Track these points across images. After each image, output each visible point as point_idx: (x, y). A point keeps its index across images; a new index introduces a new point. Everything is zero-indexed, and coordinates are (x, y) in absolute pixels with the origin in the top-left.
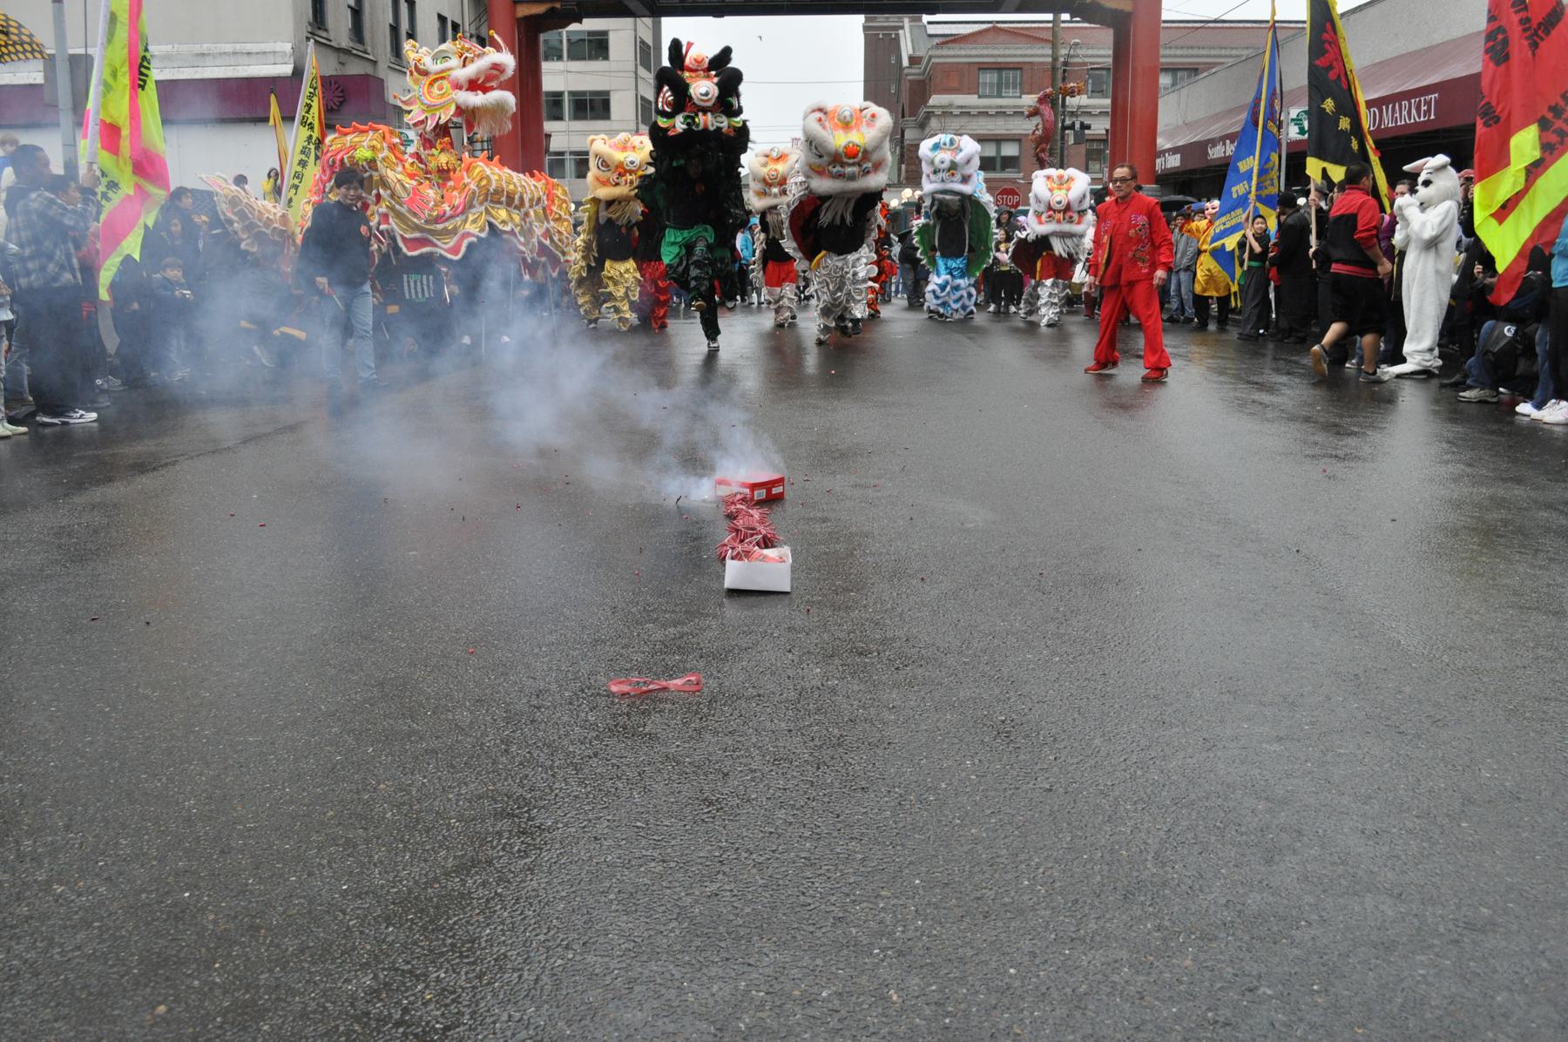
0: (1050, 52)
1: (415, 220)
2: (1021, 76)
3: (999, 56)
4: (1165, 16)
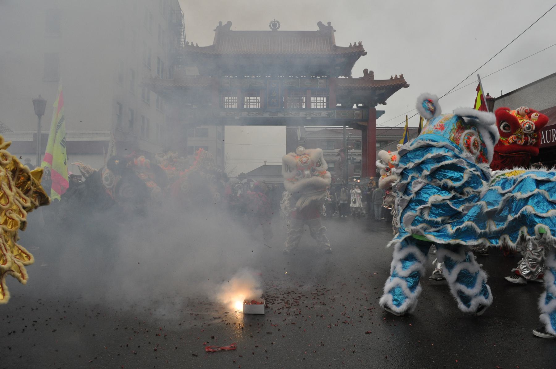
0: (342, 136)
4: (377, 127)
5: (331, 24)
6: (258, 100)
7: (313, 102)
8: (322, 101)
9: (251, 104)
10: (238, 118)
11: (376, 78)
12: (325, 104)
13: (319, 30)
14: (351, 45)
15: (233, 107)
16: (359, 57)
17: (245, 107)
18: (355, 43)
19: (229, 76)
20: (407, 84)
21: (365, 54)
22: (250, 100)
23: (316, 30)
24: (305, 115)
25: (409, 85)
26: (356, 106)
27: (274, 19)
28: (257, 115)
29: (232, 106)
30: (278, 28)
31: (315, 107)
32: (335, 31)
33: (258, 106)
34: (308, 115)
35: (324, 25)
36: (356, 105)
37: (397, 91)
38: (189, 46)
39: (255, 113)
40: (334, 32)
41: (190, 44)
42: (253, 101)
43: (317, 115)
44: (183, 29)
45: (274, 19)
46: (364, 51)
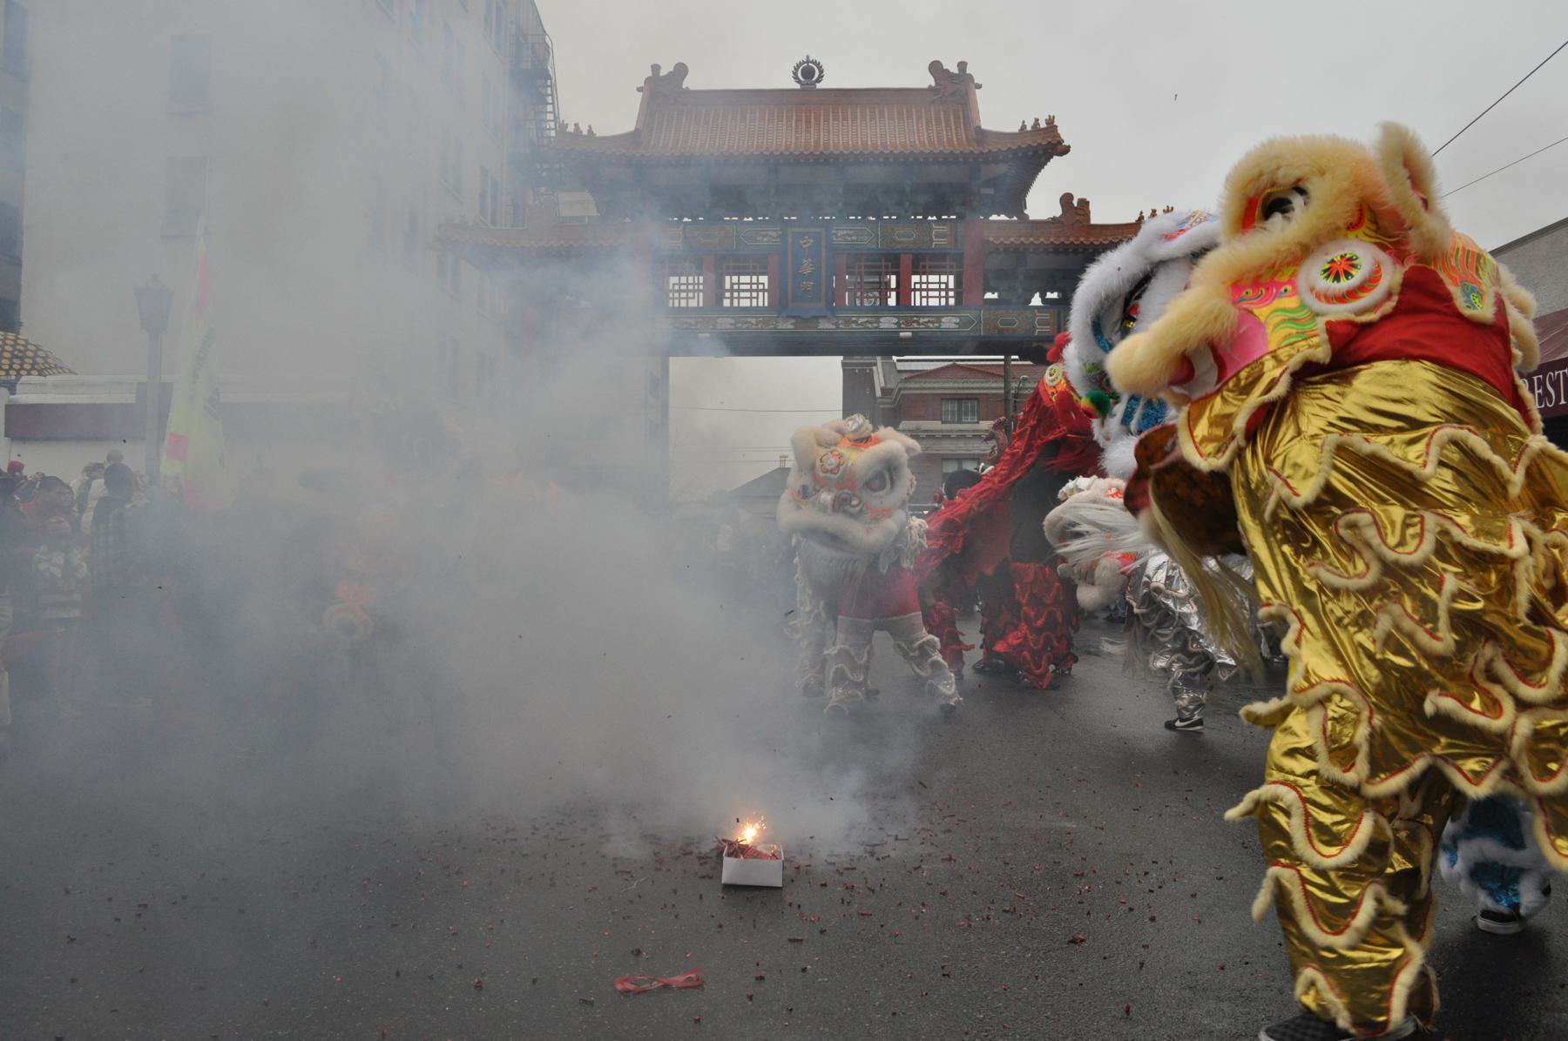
0: (1003, 385)
2: (978, 403)
3: (959, 388)
5: (968, 66)
6: (763, 284)
7: (918, 290)
8: (943, 286)
9: (742, 294)
11: (1095, 219)
12: (951, 294)
13: (933, 84)
14: (1024, 127)
15: (693, 303)
16: (1048, 160)
17: (727, 303)
18: (1037, 120)
19: (681, 218)
21: (1066, 150)
22: (739, 284)
23: (926, 86)
24: (896, 326)
27: (808, 57)
28: (760, 326)
29: (690, 300)
30: (818, 80)
31: (924, 304)
32: (979, 86)
33: (763, 300)
34: (902, 326)
35: (947, 71)
36: (1040, 296)
38: (570, 133)
39: (753, 321)
40: (977, 91)
41: (571, 129)
42: (748, 287)
43: (931, 325)
44: (551, 86)
45: (808, 57)
46: (1060, 142)
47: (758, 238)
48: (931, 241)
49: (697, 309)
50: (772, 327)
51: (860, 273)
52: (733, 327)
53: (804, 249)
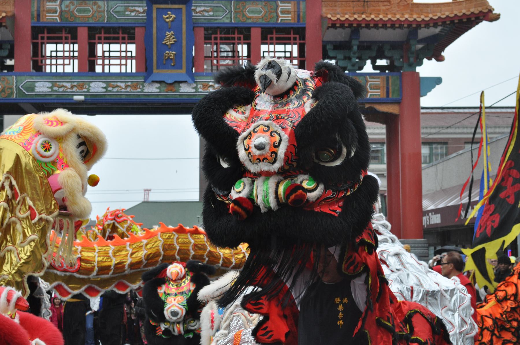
1: (14, 183)
6: (131, 52)
9: (112, 62)
10: (82, 98)
15: (69, 69)
17: (98, 69)
20: (494, 12)
25: (499, 15)
26: (371, 66)
28: (128, 89)
33: (131, 67)
37: (470, 28)
39: (123, 85)
42: (118, 54)
47: (127, 13)
48: (278, 17)
49: (73, 74)
50: (139, 90)
51: (216, 44)
52: (104, 90)
53: (168, 22)
